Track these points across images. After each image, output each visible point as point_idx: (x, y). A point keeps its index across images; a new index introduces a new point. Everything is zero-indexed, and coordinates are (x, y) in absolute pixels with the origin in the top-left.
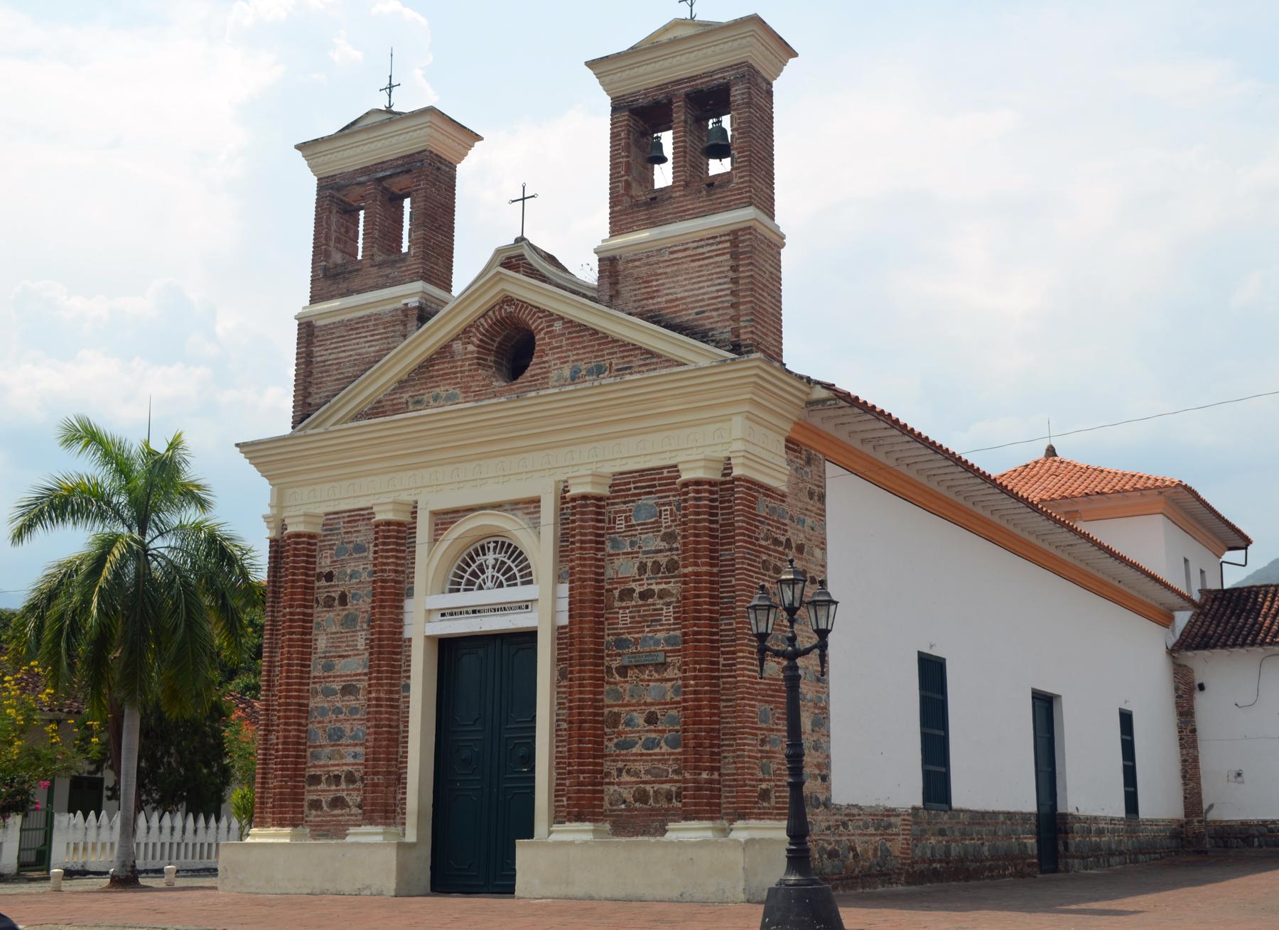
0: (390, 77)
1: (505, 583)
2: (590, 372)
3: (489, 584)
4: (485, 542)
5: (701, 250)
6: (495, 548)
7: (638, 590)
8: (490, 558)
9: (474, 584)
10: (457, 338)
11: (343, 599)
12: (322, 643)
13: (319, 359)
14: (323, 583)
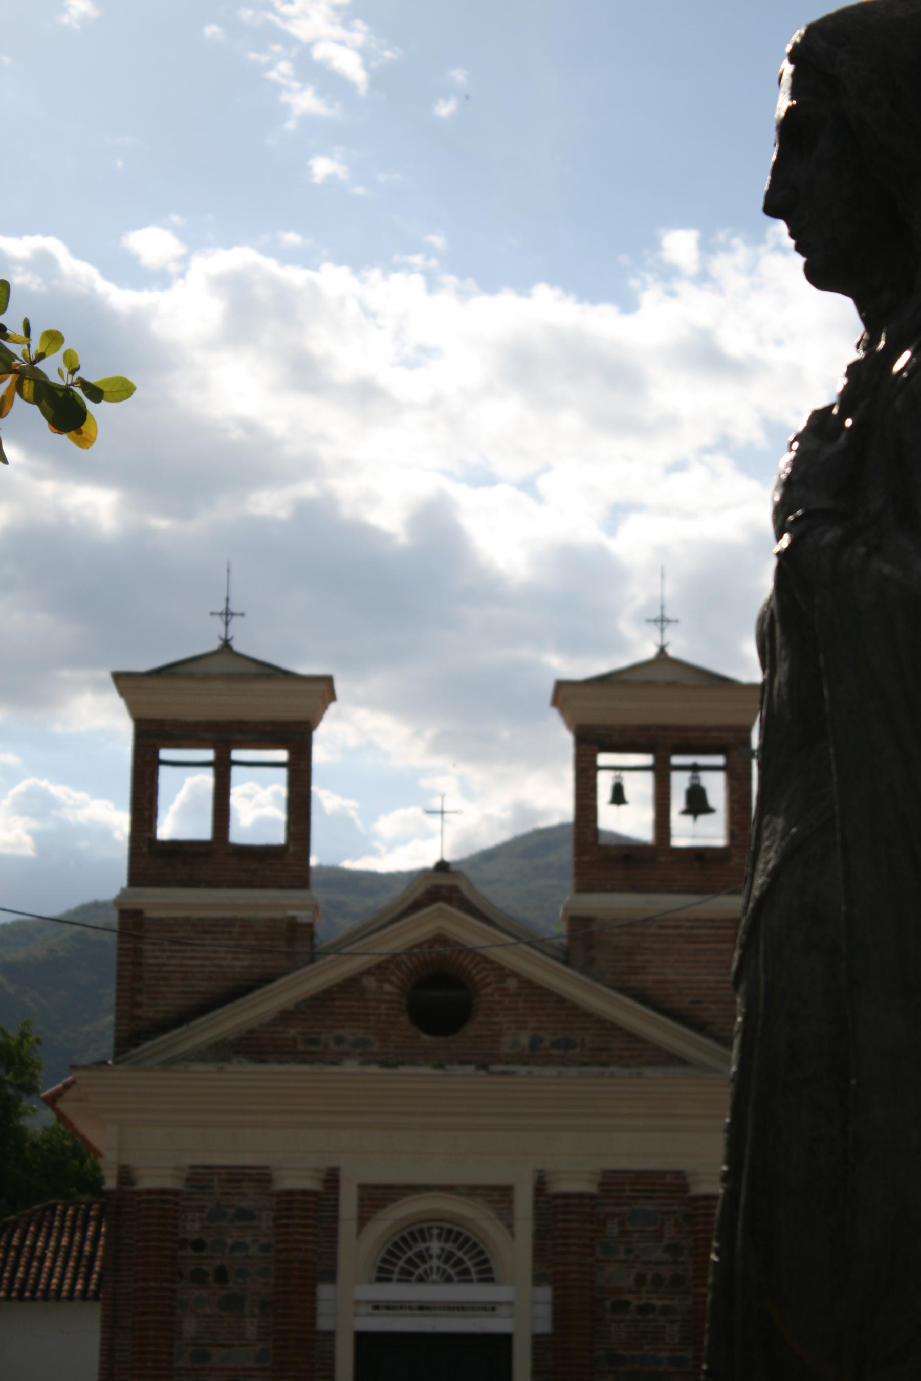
0: (227, 600)
1: (455, 1278)
2: (556, 1045)
3: (435, 1276)
4: (425, 1226)
5: (696, 932)
6: (440, 1236)
7: (635, 1303)
8: (435, 1246)
9: (411, 1274)
10: (368, 972)
11: (222, 1275)
12: (189, 1326)
13: (151, 961)
14: (189, 1252)
